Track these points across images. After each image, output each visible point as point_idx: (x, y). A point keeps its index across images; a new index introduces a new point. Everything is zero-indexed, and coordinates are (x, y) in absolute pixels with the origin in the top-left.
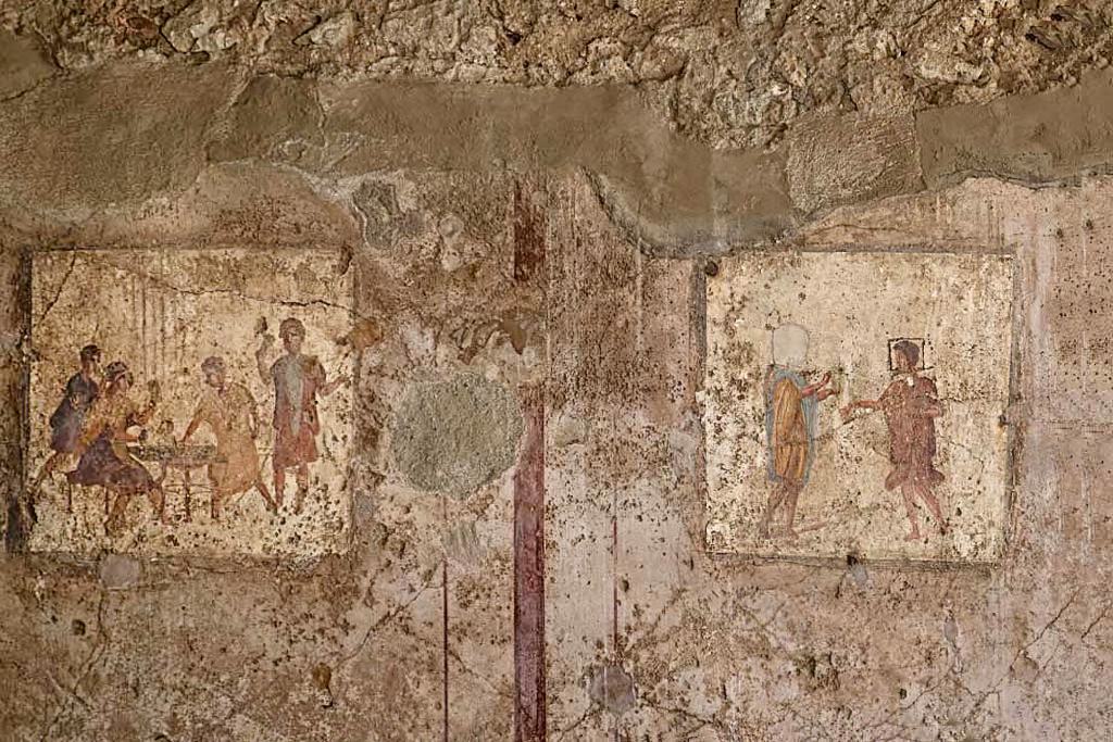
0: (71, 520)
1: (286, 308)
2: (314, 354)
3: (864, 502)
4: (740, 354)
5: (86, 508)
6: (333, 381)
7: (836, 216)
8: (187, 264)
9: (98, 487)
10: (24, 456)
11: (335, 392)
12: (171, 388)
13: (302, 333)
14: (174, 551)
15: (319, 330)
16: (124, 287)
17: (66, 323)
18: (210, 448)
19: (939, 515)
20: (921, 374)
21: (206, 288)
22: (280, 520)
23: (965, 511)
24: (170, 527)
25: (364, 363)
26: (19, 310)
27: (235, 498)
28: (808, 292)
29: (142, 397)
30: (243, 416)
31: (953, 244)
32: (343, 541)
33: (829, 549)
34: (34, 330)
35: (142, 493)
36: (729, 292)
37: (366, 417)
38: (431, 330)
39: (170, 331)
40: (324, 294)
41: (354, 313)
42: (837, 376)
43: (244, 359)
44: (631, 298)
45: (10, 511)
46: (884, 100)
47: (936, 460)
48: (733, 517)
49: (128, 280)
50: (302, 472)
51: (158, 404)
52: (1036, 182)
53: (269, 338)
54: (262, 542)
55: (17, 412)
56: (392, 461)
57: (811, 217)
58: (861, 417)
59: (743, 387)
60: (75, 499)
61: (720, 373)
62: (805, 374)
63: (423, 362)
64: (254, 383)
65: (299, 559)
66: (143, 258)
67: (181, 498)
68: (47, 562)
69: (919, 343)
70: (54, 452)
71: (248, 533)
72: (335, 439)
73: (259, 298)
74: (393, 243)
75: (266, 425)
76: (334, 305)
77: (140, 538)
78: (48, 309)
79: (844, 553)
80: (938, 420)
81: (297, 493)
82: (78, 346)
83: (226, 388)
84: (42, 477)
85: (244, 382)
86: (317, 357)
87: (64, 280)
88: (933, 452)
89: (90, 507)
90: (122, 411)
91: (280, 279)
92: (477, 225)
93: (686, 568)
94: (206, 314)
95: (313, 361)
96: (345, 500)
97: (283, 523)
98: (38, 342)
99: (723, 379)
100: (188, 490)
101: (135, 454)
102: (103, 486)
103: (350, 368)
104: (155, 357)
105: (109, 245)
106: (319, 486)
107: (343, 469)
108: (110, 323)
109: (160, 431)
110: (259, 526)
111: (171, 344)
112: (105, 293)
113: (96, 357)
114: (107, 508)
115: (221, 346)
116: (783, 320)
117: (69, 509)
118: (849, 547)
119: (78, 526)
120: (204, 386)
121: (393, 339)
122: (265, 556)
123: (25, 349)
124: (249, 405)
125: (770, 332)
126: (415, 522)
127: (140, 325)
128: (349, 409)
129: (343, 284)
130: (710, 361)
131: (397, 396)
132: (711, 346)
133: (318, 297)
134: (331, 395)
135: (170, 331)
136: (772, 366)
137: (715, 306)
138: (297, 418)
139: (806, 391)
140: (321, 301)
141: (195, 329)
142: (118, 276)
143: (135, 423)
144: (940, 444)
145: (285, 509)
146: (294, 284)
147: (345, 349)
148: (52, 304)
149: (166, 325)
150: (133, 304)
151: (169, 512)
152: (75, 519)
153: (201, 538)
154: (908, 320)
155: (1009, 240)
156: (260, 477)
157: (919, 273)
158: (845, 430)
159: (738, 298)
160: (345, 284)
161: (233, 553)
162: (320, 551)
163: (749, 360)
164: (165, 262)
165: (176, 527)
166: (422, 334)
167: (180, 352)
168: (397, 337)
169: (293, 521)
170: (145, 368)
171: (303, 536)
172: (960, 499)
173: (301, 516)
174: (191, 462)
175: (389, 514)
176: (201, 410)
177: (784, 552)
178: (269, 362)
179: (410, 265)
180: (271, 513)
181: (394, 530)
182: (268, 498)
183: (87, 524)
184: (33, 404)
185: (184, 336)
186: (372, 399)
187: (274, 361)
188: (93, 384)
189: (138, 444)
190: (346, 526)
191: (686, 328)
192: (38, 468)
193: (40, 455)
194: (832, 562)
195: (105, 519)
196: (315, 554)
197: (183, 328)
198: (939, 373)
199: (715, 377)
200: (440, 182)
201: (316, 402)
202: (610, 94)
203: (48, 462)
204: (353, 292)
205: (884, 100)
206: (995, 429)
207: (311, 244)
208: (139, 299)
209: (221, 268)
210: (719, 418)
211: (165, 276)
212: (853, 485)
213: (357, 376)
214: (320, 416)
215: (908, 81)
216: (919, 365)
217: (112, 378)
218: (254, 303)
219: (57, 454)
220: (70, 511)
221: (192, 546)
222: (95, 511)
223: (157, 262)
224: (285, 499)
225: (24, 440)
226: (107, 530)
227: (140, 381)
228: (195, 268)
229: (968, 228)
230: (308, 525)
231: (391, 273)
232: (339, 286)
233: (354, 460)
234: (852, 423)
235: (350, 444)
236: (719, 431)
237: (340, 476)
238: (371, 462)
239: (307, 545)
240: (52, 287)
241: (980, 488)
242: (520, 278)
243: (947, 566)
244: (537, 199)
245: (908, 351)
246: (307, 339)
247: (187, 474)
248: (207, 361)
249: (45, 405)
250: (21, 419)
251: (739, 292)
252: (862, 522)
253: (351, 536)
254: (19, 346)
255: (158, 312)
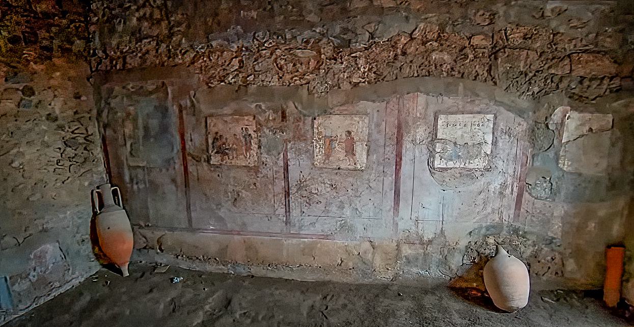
4: (319, 133)
7: (337, 108)
31: (357, 113)
44: (301, 124)
46: (346, 86)
52: (374, 101)
57: (332, 109)
64: (242, 138)
92: (275, 112)
129: (254, 121)
131: (264, 140)
175: (264, 160)
194: (336, 169)
200: (269, 104)
202: (297, 87)
205: (346, 86)
215: (350, 83)
223: (225, 119)
229: (360, 110)
242: (282, 121)
244: (285, 107)
245: (349, 132)
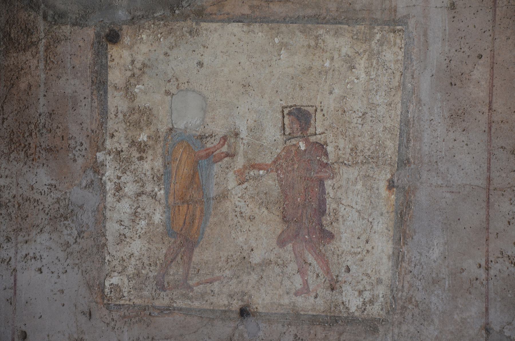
3: (256, 258)
19: (328, 272)
20: (313, 139)
23: (353, 268)
28: (206, 60)
33: (222, 301)
36: (129, 59)
42: (232, 140)
47: (326, 220)
48: (131, 270)
58: (255, 178)
59: (142, 148)
61: (121, 135)
62: (201, 137)
69: (311, 110)
79: (236, 305)
80: (328, 183)
88: (323, 212)
93: (83, 319)
99: (123, 140)
116: (182, 87)
118: (242, 300)
125: (169, 97)
130: (110, 124)
132: (112, 109)
136: (171, 129)
137: (117, 73)
139: (203, 154)
144: (330, 205)
154: (301, 88)
155: (402, 11)
157: (313, 43)
158: (239, 190)
159: (139, 65)
163: (149, 123)
172: (349, 258)
177: (180, 303)
191: (88, 92)
198: (330, 137)
199: (115, 139)
206: (384, 192)
210: (119, 178)
212: (246, 241)
216: (311, 130)
234: (246, 184)
236: (119, 188)
241: (369, 247)
243: (335, 320)
251: (140, 58)
252: (254, 277)
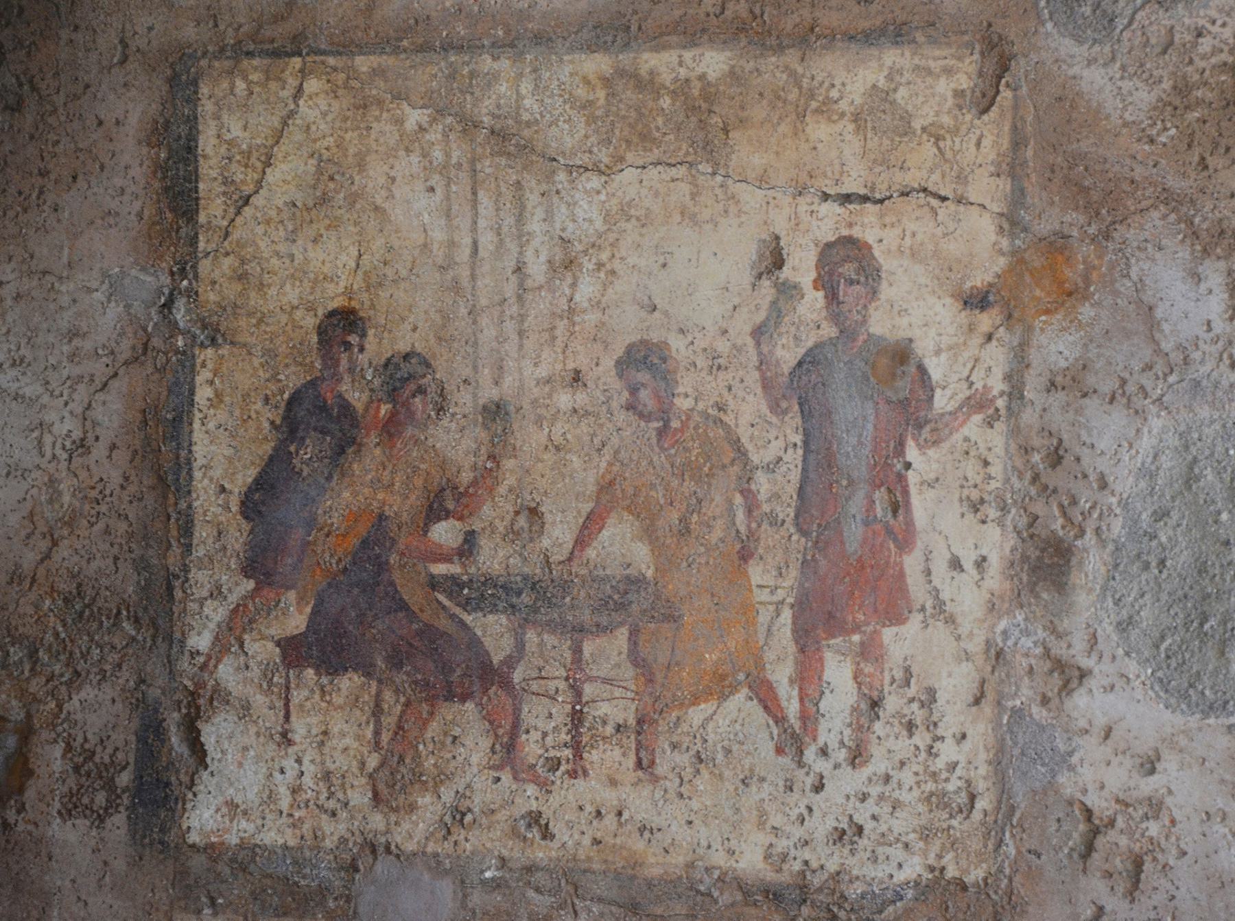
0: (290, 764)
1: (830, 209)
2: (902, 334)
5: (325, 733)
6: (949, 408)
8: (581, 92)
9: (357, 679)
10: (178, 594)
11: (957, 437)
12: (539, 422)
13: (869, 273)
14: (541, 853)
15: (918, 269)
16: (425, 155)
17: (282, 248)
18: (636, 582)
21: (630, 157)
22: (809, 781)
24: (531, 790)
25: (1034, 356)
26: (169, 215)
27: (696, 715)
29: (468, 443)
30: (718, 499)
32: (975, 844)
34: (205, 266)
35: (464, 698)
37: (1038, 508)
38: (1222, 265)
39: (537, 269)
40: (931, 171)
41: (1011, 222)
43: (723, 346)
45: (141, 739)
49: (434, 135)
50: (870, 652)
51: (509, 464)
53: (788, 291)
54: (763, 838)
55: (161, 479)
56: (1107, 629)
60: (301, 706)
63: (1197, 355)
65: (859, 888)
66: (472, 75)
67: (561, 712)
68: (227, 871)
70: (251, 584)
71: (729, 812)
72: (956, 564)
73: (763, 181)
74: (1121, 23)
75: (776, 523)
76: (959, 201)
77: (459, 814)
78: (238, 213)
81: (854, 709)
82: (311, 309)
83: (675, 424)
84: (221, 647)
85: (721, 408)
86: (911, 340)
87: (278, 136)
89: (335, 730)
90: (419, 482)
91: (819, 130)
94: (629, 226)
95: (901, 354)
96: (980, 731)
97: (819, 788)
98: (212, 297)
100: (578, 694)
101: (450, 596)
102: (368, 675)
103: (998, 373)
104: (501, 339)
105: (387, 44)
106: (912, 691)
107: (975, 646)
108: (390, 249)
109: (513, 533)
110: (756, 794)
111: (540, 306)
112: (377, 172)
113: (354, 339)
114: (377, 733)
115: (666, 313)
117: (284, 734)
119: (308, 781)
120: (621, 417)
121: (1116, 293)
122: (770, 876)
123: (180, 314)
124: (735, 470)
126: (1169, 801)
127: (464, 254)
128: (994, 485)
133: (913, 178)
134: (946, 446)
135: (537, 269)
138: (856, 506)
140: (925, 190)
141: (600, 265)
142: (410, 124)
143: (448, 515)
145: (824, 752)
146: (852, 146)
147: (986, 321)
148: (247, 201)
149: (529, 255)
150: (448, 198)
151: (531, 748)
152: (299, 761)
153: (610, 820)
156: (760, 664)
160: (986, 142)
161: (690, 865)
162: (913, 868)
164: (526, 87)
165: (546, 787)
166: (1197, 278)
167: (562, 325)
168: (1124, 286)
169: (844, 783)
170: (475, 368)
171: (869, 826)
173: (867, 771)
174: (586, 617)
176: (611, 483)
178: (787, 355)
179: (1167, 85)
180: (786, 761)
181: (1112, 823)
182: (780, 719)
183: (327, 776)
184: (200, 461)
185: (574, 285)
186: (1056, 458)
187: (801, 351)
188: (346, 408)
189: (455, 569)
190: (980, 804)
192: (212, 626)
193: (217, 593)
195: (373, 762)
196: (900, 877)
197: (570, 264)
201: (908, 466)
203: (235, 611)
204: (1012, 167)
207: (898, 33)
208: (461, 187)
209: (666, 102)
211: (528, 124)
213: (1015, 392)
214: (916, 500)
217: (393, 394)
218: (751, 197)
219: (257, 589)
220: (286, 739)
221: (587, 841)
222: (348, 741)
224: (823, 725)
225: (176, 550)
226: (376, 796)
227: (463, 401)
228: (602, 102)
230: (881, 797)
231: (1112, 105)
232: (973, 149)
233: (1003, 624)
235: (994, 580)
237: (966, 667)
238: (1053, 630)
239: (880, 850)
240: (248, 155)
246: (886, 292)
247: (577, 650)
248: (630, 349)
249: (230, 460)
250: (172, 500)
253: (995, 831)
254: (169, 305)
255: (510, 220)
